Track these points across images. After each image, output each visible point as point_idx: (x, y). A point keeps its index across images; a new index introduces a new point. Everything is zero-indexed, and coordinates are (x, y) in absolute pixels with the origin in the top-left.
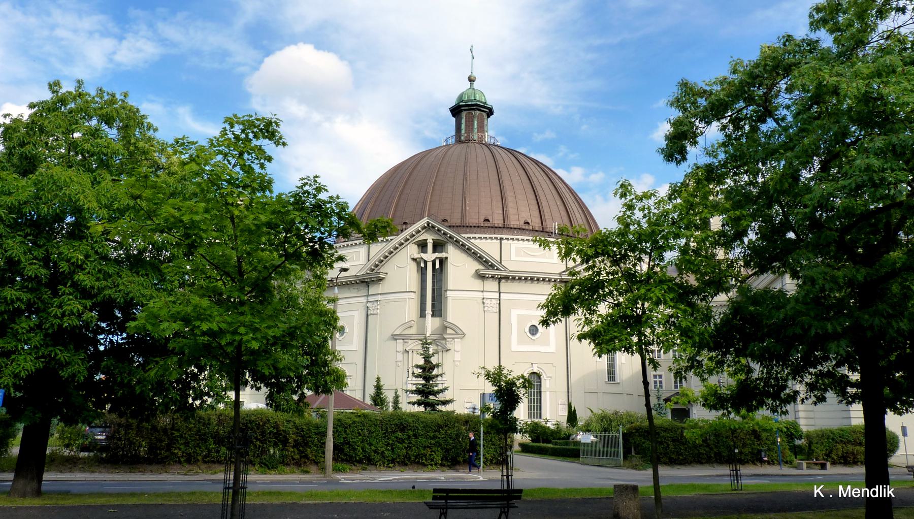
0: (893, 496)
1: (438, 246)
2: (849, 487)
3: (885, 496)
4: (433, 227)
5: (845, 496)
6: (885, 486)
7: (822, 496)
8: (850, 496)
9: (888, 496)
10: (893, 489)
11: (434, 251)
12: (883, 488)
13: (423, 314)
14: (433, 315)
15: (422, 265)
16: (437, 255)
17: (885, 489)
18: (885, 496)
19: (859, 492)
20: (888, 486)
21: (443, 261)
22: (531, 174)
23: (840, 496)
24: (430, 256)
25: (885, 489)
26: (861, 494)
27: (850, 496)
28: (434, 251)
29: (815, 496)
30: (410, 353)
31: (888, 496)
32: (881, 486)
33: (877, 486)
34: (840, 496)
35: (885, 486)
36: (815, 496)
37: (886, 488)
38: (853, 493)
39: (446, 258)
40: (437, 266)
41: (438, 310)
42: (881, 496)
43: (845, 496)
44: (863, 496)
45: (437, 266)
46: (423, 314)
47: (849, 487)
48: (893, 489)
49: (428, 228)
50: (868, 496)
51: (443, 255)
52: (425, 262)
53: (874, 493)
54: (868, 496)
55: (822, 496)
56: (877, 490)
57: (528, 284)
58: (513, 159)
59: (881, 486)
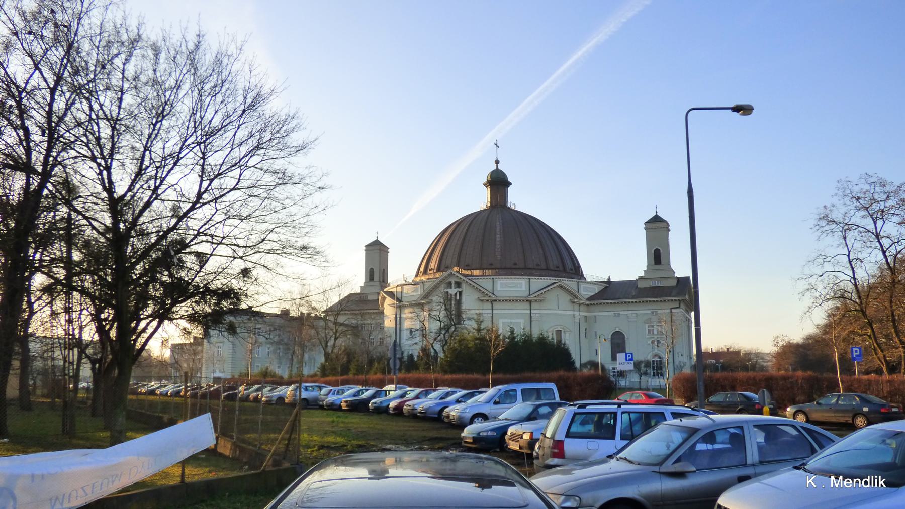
5: (837, 486)
7: (815, 486)
8: (841, 486)
10: (884, 480)
17: (876, 480)
20: (880, 477)
23: (832, 486)
25: (876, 480)
27: (841, 486)
29: (808, 486)
32: (873, 477)
33: (869, 477)
34: (832, 486)
35: (876, 477)
36: (808, 486)
43: (837, 486)
48: (884, 480)
53: (866, 483)
55: (815, 486)
59: (873, 477)
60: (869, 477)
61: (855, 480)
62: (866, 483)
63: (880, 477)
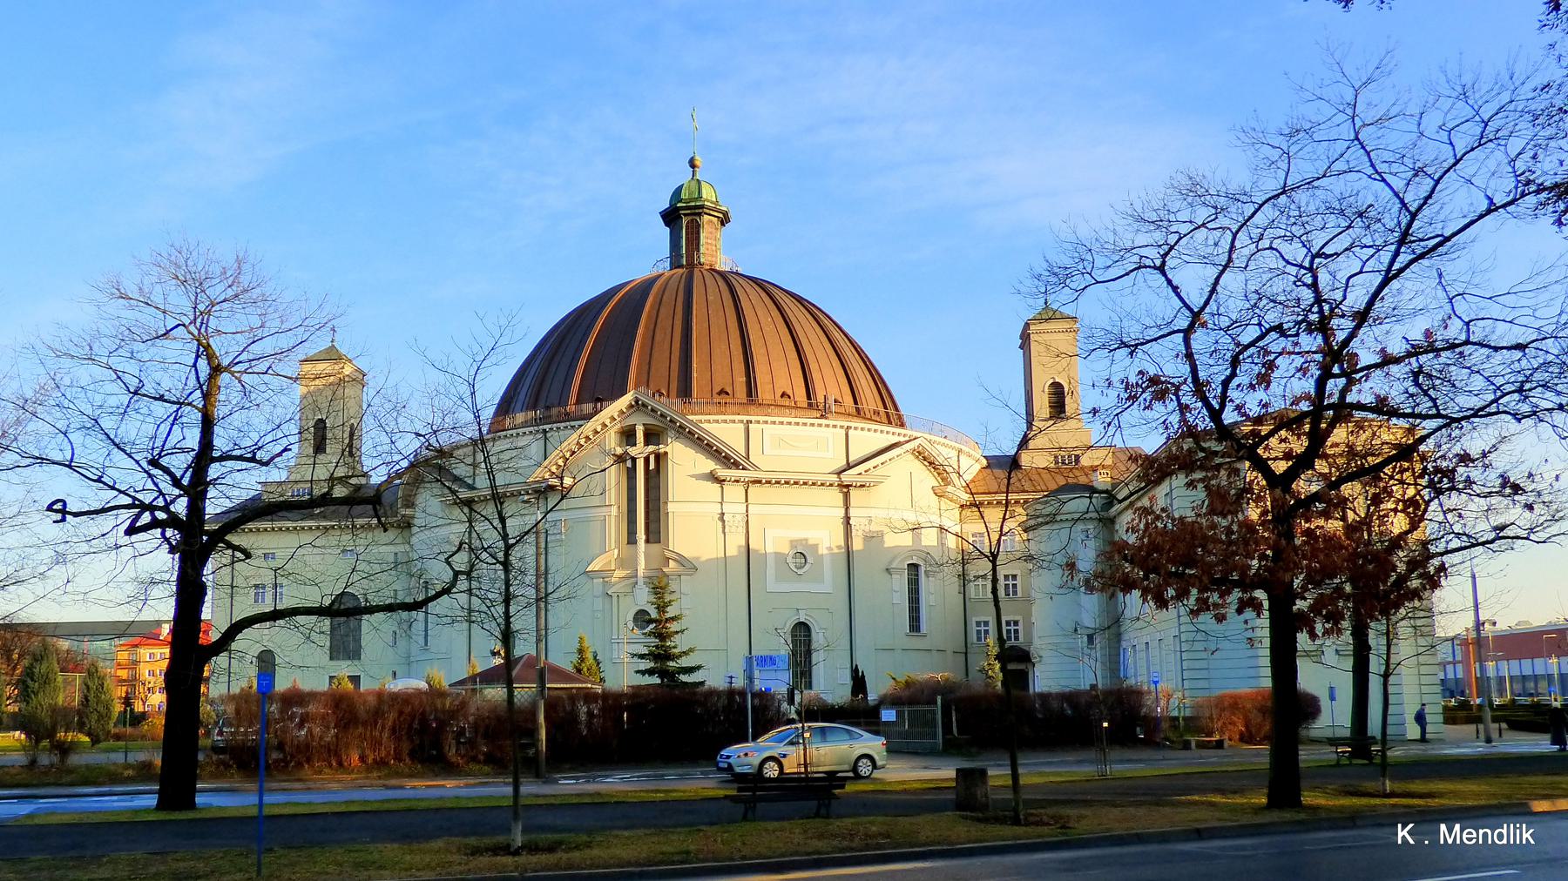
0: (1532, 842)
1: (652, 436)
2: (1457, 827)
3: (1518, 842)
4: (644, 405)
5: (1450, 841)
6: (1518, 825)
8: (1458, 842)
9: (1524, 842)
10: (1531, 831)
11: (647, 443)
12: (1515, 828)
13: (632, 540)
14: (647, 541)
15: (629, 464)
16: (651, 448)
17: (1518, 831)
18: (1518, 842)
19: (1475, 836)
20: (1524, 825)
21: (660, 458)
22: (793, 320)
23: (1442, 842)
24: (640, 450)
25: (1518, 831)
26: (1477, 838)
27: (1458, 842)
28: (647, 443)
29: (1400, 842)
30: (615, 599)
31: (1524, 842)
32: (1512, 825)
33: (1505, 825)
34: (1442, 842)
35: (1518, 825)
36: (1400, 842)
37: (1521, 828)
38: (1465, 836)
39: (666, 453)
40: (652, 466)
41: (655, 532)
42: (1512, 842)
43: (1450, 841)
44: (1481, 842)
45: (652, 466)
46: (632, 540)
47: (1457, 827)
48: (1531, 831)
49: (637, 405)
50: (1490, 842)
51: (662, 448)
52: (634, 460)
53: (1500, 836)
54: (1490, 842)
55: (1412, 842)
56: (1504, 831)
57: (815, 489)
58: (763, 295)
59: (1512, 825)
60: (1505, 825)
61: (1481, 832)
62: (1500, 836)
63: (1524, 825)
